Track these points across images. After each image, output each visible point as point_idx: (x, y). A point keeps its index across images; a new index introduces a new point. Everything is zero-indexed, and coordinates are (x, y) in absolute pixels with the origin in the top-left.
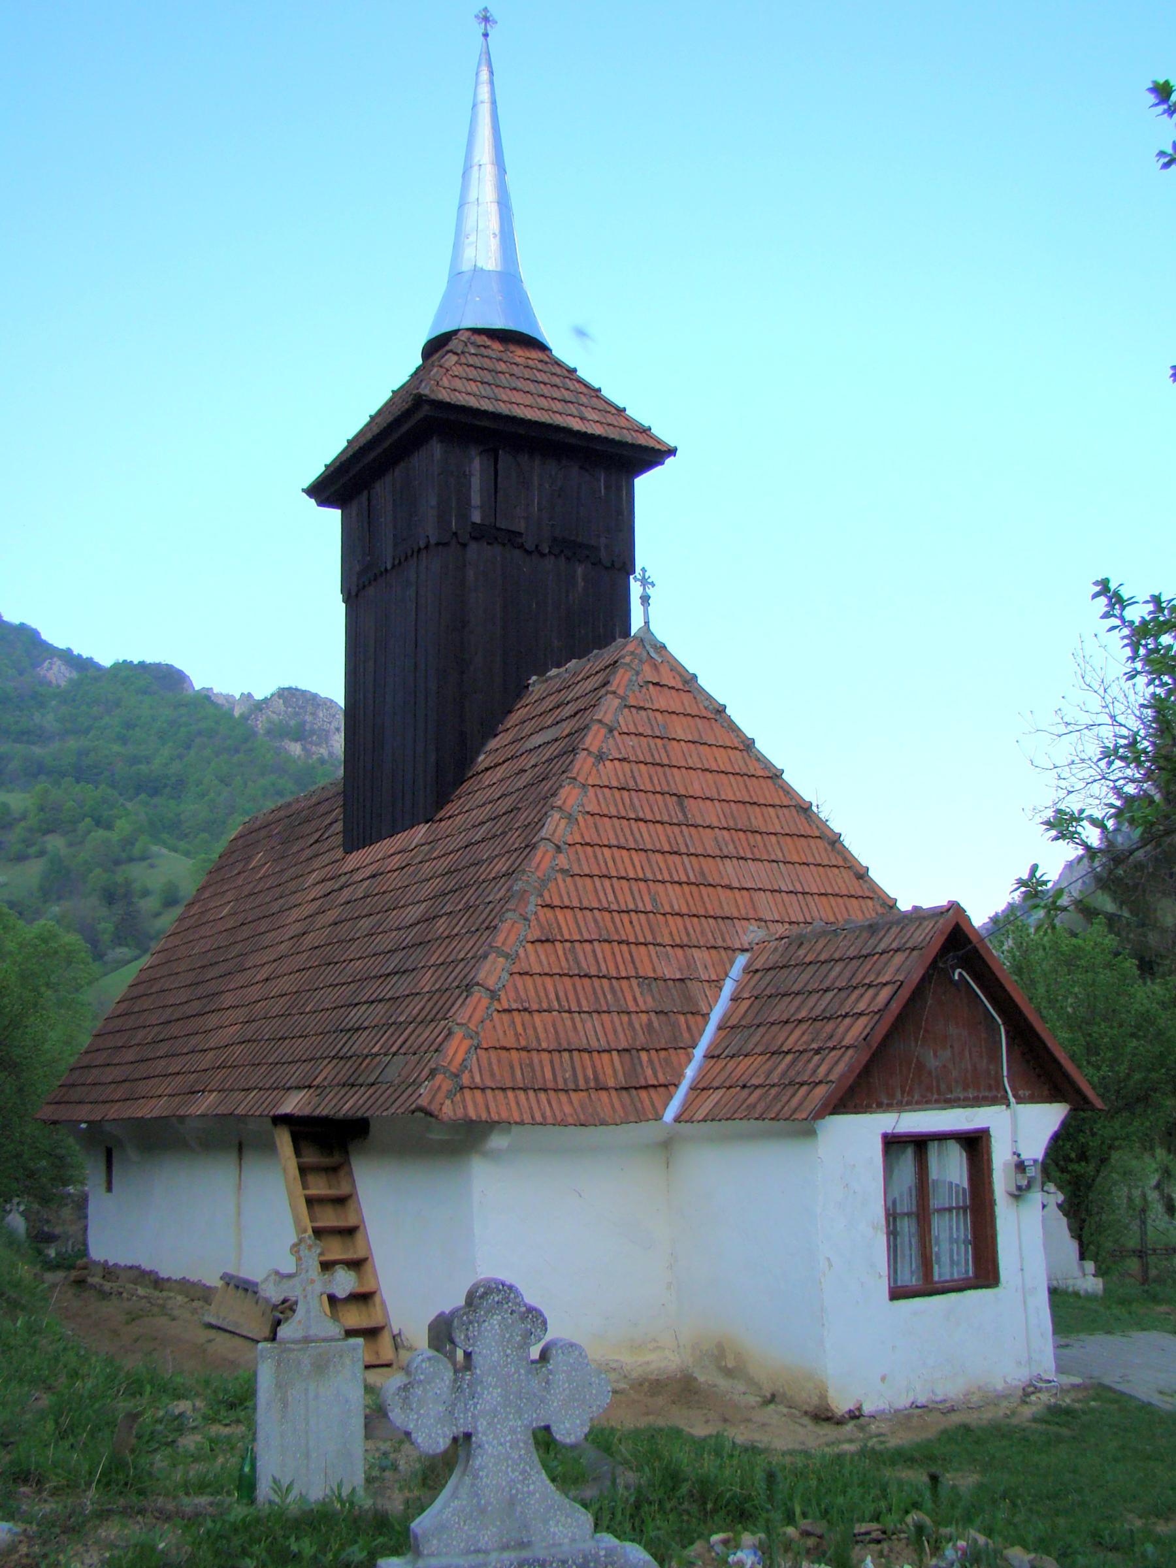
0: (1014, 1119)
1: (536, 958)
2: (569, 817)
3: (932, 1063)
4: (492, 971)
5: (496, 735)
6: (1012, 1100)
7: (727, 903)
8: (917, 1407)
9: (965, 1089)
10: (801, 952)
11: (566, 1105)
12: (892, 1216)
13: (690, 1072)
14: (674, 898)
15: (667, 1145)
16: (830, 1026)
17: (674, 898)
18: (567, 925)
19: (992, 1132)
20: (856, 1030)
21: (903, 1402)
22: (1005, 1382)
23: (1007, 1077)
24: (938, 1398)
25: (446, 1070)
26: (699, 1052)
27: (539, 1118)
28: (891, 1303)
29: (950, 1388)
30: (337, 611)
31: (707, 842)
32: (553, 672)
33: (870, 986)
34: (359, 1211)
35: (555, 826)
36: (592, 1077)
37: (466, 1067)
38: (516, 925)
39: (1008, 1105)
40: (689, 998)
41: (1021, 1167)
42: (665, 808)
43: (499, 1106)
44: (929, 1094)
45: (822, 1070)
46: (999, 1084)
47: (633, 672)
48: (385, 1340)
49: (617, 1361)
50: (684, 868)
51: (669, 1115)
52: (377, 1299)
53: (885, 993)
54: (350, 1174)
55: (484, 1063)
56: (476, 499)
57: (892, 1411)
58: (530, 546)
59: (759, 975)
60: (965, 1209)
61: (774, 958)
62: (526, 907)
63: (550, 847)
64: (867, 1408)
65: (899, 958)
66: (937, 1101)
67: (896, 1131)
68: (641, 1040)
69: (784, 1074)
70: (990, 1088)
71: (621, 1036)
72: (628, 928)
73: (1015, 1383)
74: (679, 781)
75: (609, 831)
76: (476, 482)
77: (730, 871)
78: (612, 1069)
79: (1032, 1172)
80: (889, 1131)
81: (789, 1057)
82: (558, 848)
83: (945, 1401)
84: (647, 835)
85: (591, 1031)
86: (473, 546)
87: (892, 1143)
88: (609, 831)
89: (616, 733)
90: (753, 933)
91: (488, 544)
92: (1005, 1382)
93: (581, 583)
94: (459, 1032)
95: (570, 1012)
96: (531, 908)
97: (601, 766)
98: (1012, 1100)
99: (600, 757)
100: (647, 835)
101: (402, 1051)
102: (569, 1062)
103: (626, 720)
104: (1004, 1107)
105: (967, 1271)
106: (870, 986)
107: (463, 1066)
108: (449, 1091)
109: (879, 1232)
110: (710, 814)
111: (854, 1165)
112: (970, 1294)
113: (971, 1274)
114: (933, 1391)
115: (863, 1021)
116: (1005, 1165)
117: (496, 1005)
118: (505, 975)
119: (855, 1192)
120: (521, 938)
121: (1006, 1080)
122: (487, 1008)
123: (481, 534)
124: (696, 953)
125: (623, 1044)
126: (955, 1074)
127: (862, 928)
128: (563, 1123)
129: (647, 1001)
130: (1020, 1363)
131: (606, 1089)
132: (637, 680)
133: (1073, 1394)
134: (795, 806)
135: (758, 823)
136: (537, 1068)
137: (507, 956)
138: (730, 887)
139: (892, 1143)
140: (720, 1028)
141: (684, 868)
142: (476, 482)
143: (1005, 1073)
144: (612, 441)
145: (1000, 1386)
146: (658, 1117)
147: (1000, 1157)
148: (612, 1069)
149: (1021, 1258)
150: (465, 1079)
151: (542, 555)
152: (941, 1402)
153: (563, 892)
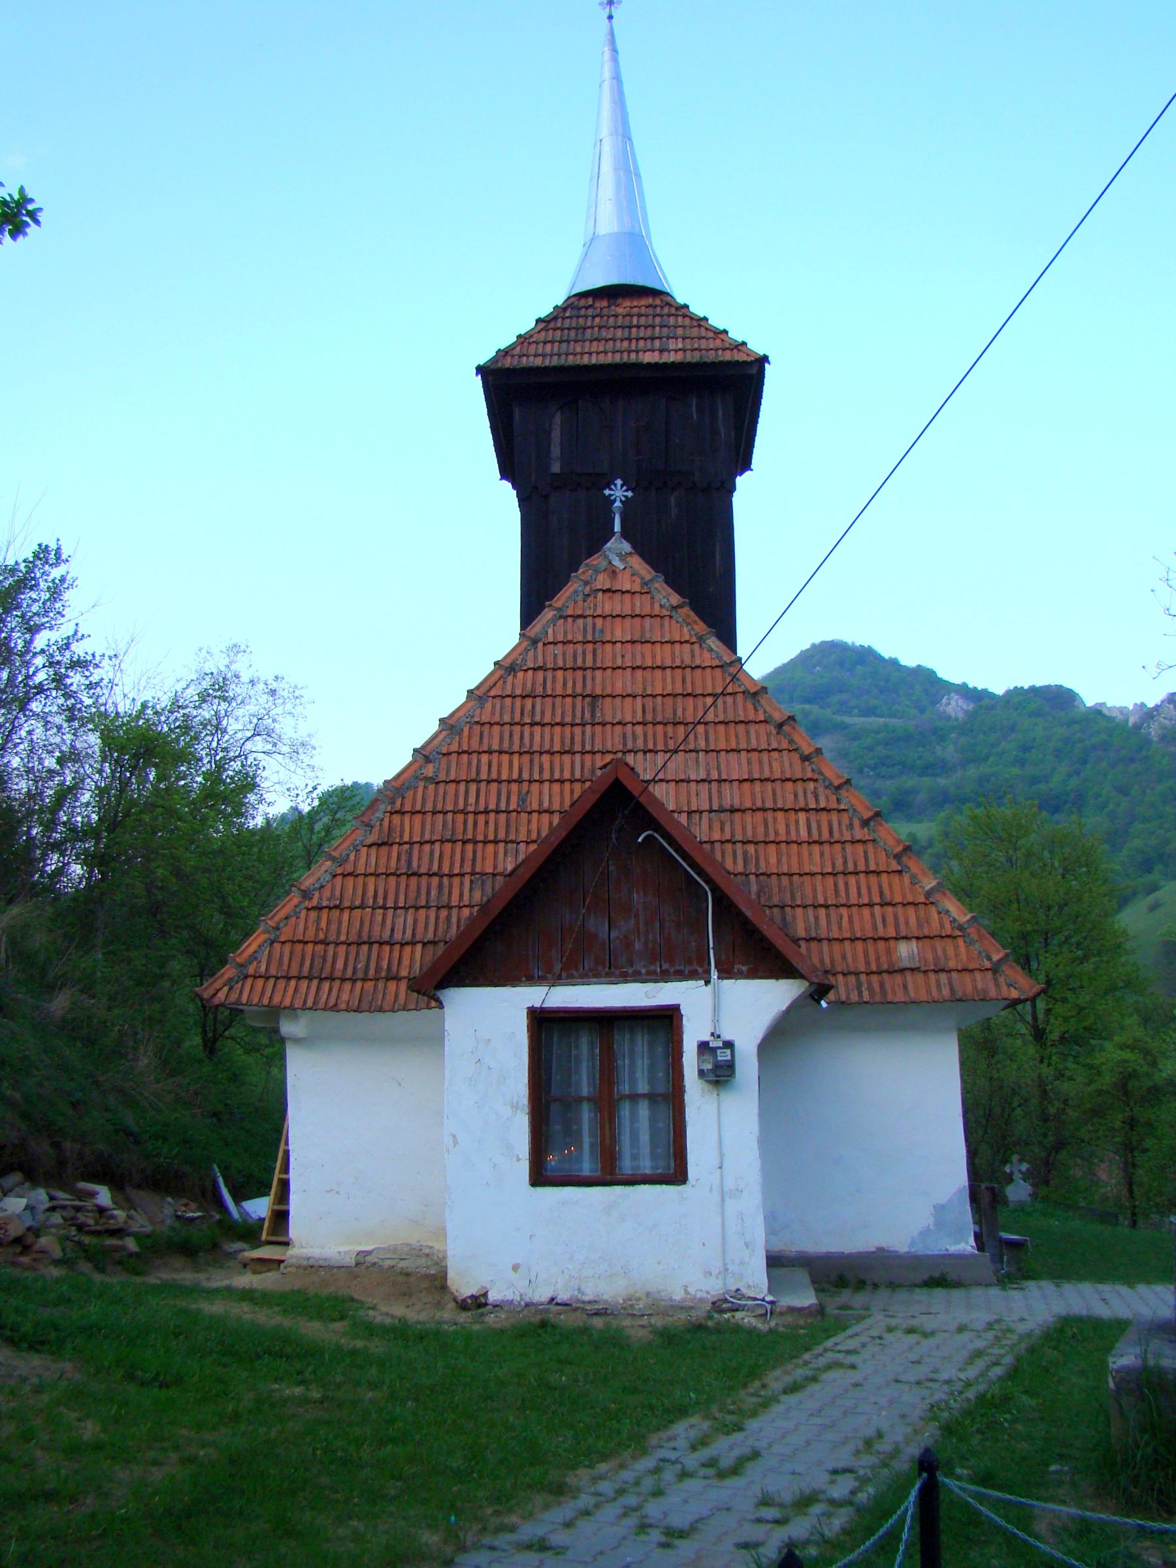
0: (716, 996)
6: (714, 974)
8: (558, 1304)
9: (653, 961)
19: (682, 1012)
21: (541, 1294)
22: (687, 1292)
23: (713, 948)
24: (586, 1298)
27: (310, 1003)
28: (532, 1188)
36: (386, 967)
37: (256, 959)
38: (357, 832)
39: (707, 982)
43: (284, 994)
44: (600, 968)
46: (703, 959)
47: (582, 583)
49: (431, 1247)
55: (276, 955)
56: (556, 451)
57: (523, 1303)
62: (373, 814)
66: (608, 975)
67: (547, 1005)
70: (689, 961)
71: (431, 928)
73: (699, 1295)
76: (556, 434)
78: (414, 961)
80: (537, 1005)
83: (596, 1302)
85: (403, 924)
89: (540, 645)
91: (571, 490)
92: (687, 1292)
93: (674, 511)
95: (384, 908)
96: (379, 814)
97: (510, 678)
98: (714, 974)
102: (366, 954)
104: (702, 982)
105: (669, 1167)
107: (254, 957)
108: (231, 979)
109: (519, 1111)
111: (489, 1040)
113: (672, 1171)
114: (579, 1289)
117: (306, 904)
118: (328, 877)
119: (489, 1068)
120: (358, 842)
121: (711, 952)
122: (296, 906)
126: (638, 946)
128: (335, 1008)
130: (711, 1274)
132: (583, 591)
133: (789, 1319)
134: (743, 693)
136: (330, 959)
143: (711, 945)
144: (690, 365)
145: (678, 1296)
149: (722, 1156)
152: (590, 1302)
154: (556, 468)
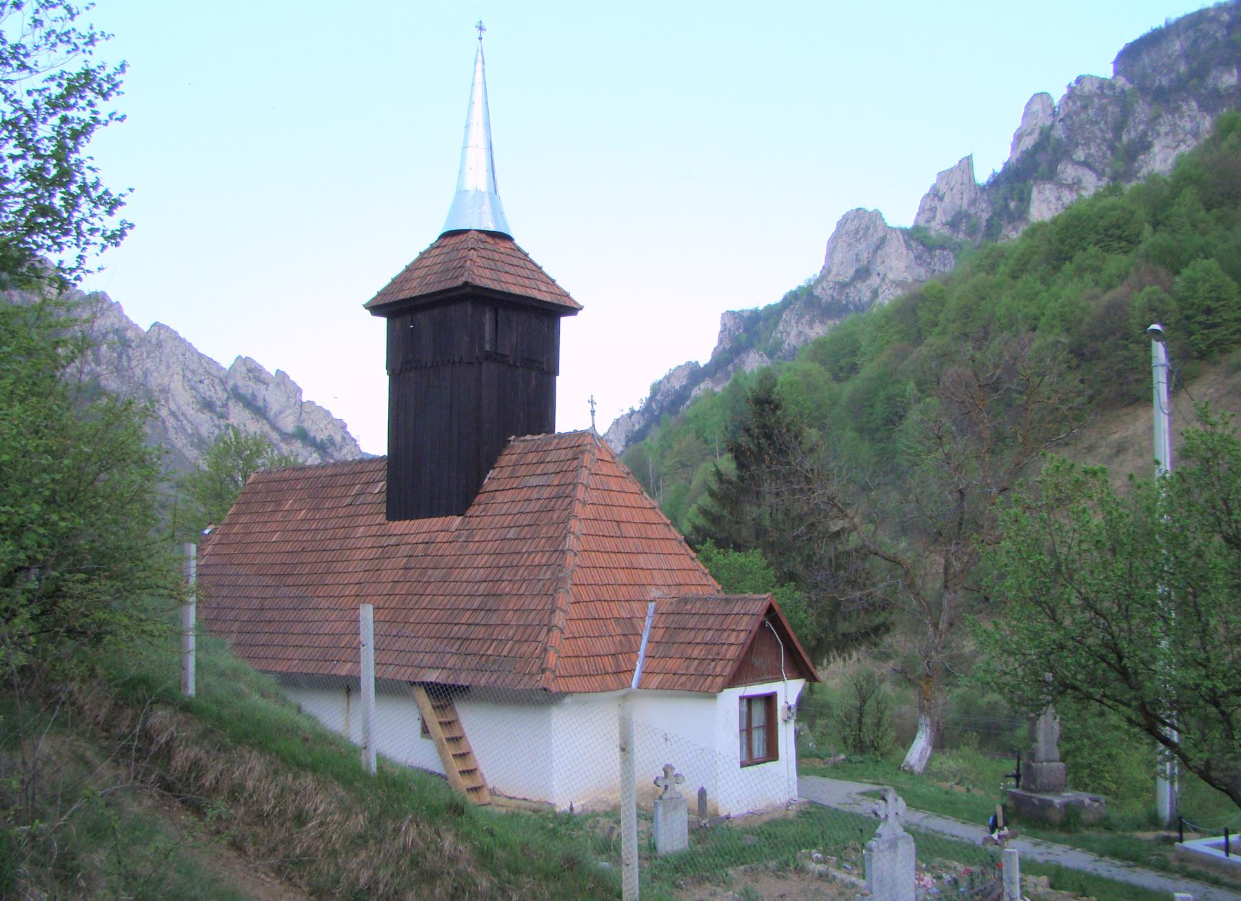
1: (575, 612)
2: (578, 538)
3: (757, 664)
4: (559, 619)
5: (493, 468)
7: (643, 577)
10: (689, 607)
11: (596, 682)
12: (741, 731)
13: (638, 664)
14: (622, 576)
15: (624, 697)
16: (716, 648)
17: (622, 576)
18: (584, 594)
20: (732, 652)
21: (745, 810)
25: (550, 669)
26: (641, 653)
29: (761, 805)
30: (383, 380)
31: (632, 545)
32: (528, 437)
33: (733, 630)
34: (461, 729)
35: (571, 542)
40: (634, 627)
41: (789, 708)
42: (612, 529)
45: (718, 670)
48: (485, 792)
50: (623, 560)
51: (634, 684)
52: (478, 774)
53: (743, 636)
54: (453, 709)
58: (511, 363)
59: (664, 616)
60: (763, 727)
61: (671, 609)
63: (572, 554)
64: (732, 815)
65: (746, 618)
68: (619, 649)
69: (696, 669)
70: (777, 674)
72: (606, 593)
74: (618, 514)
75: (593, 544)
77: (642, 560)
79: (794, 710)
81: (696, 662)
82: (575, 554)
84: (610, 544)
85: (600, 646)
86: (485, 363)
87: (749, 700)
88: (593, 544)
90: (654, 593)
94: (552, 651)
96: (569, 586)
99: (584, 503)
100: (610, 544)
101: (512, 655)
103: (591, 481)
106: (733, 630)
110: (630, 530)
112: (768, 763)
115: (733, 648)
116: (783, 708)
123: (489, 357)
124: (634, 604)
125: (613, 652)
127: (721, 599)
129: (619, 631)
131: (608, 673)
135: (650, 535)
137: (564, 611)
138: (642, 569)
139: (741, 698)
140: (649, 641)
141: (623, 560)
142: (487, 327)
146: (630, 686)
147: (780, 704)
148: (609, 663)
150: (557, 673)
151: (515, 366)
153: (580, 576)
154: (487, 347)
